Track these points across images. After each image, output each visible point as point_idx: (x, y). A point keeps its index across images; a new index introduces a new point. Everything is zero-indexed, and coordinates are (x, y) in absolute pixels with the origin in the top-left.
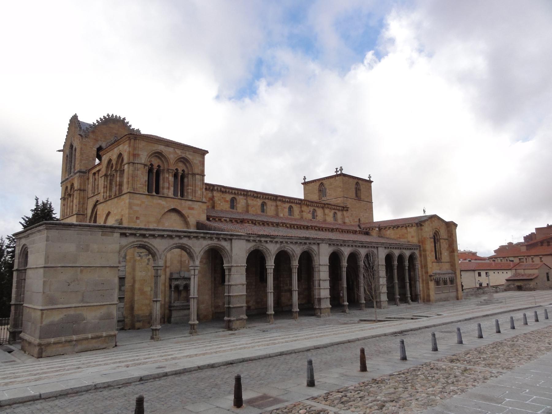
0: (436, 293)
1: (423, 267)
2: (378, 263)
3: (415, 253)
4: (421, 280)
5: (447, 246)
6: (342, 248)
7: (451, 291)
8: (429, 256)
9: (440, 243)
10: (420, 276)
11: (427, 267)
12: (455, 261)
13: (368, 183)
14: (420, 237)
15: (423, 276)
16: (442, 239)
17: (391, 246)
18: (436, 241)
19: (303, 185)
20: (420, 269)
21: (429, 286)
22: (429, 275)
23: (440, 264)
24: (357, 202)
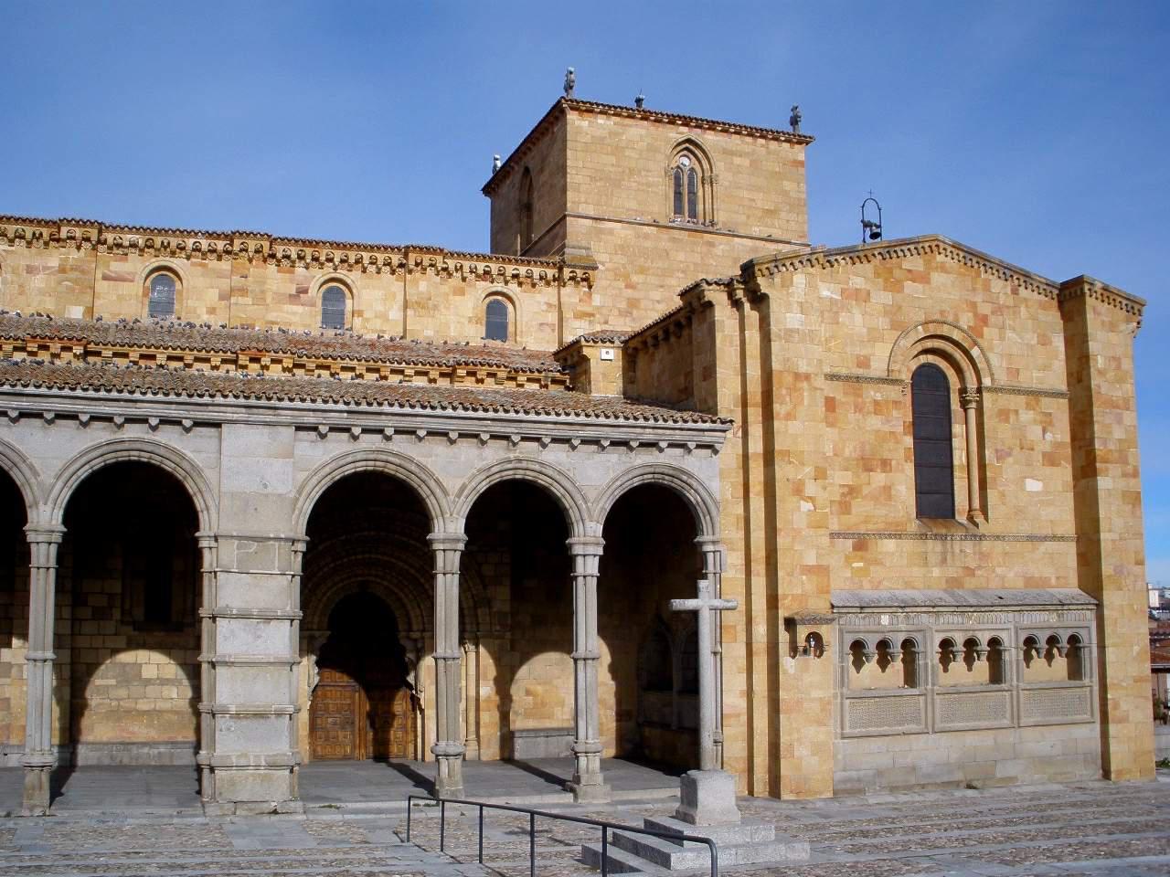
8: (798, 490)
12: (1097, 531)
13: (773, 145)
16: (989, 390)
19: (488, 200)
24: (674, 240)
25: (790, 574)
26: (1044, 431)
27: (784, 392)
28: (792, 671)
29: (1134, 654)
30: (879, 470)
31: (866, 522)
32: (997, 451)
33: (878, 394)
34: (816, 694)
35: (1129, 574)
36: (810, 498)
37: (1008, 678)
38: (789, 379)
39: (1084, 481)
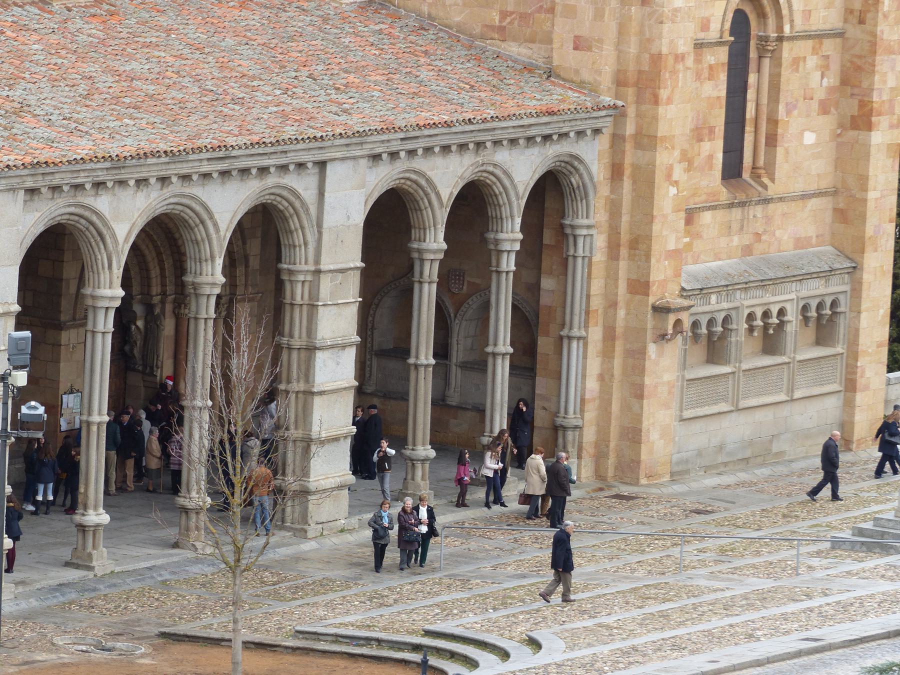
0: (687, 414)
1: (624, 252)
2: (317, 261)
3: (577, 158)
4: (595, 334)
5: (831, 80)
6: (103, 203)
7: (798, 394)
8: (669, 176)
9: (777, 63)
10: (597, 303)
11: (648, 256)
12: (864, 189)
14: (633, 49)
15: (612, 305)
17: (410, 146)
18: (753, 54)
20: (599, 257)
21: (642, 371)
22: (652, 300)
23: (758, 211)
25: (658, 261)
26: (822, 77)
27: (667, 75)
28: (653, 356)
29: (880, 318)
30: (706, 140)
31: (694, 195)
32: (787, 104)
33: (713, 58)
34: (667, 377)
35: (884, 233)
36: (676, 182)
37: (788, 350)
38: (671, 60)
39: (852, 134)
